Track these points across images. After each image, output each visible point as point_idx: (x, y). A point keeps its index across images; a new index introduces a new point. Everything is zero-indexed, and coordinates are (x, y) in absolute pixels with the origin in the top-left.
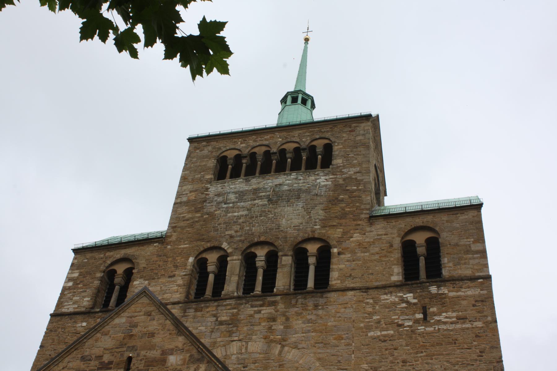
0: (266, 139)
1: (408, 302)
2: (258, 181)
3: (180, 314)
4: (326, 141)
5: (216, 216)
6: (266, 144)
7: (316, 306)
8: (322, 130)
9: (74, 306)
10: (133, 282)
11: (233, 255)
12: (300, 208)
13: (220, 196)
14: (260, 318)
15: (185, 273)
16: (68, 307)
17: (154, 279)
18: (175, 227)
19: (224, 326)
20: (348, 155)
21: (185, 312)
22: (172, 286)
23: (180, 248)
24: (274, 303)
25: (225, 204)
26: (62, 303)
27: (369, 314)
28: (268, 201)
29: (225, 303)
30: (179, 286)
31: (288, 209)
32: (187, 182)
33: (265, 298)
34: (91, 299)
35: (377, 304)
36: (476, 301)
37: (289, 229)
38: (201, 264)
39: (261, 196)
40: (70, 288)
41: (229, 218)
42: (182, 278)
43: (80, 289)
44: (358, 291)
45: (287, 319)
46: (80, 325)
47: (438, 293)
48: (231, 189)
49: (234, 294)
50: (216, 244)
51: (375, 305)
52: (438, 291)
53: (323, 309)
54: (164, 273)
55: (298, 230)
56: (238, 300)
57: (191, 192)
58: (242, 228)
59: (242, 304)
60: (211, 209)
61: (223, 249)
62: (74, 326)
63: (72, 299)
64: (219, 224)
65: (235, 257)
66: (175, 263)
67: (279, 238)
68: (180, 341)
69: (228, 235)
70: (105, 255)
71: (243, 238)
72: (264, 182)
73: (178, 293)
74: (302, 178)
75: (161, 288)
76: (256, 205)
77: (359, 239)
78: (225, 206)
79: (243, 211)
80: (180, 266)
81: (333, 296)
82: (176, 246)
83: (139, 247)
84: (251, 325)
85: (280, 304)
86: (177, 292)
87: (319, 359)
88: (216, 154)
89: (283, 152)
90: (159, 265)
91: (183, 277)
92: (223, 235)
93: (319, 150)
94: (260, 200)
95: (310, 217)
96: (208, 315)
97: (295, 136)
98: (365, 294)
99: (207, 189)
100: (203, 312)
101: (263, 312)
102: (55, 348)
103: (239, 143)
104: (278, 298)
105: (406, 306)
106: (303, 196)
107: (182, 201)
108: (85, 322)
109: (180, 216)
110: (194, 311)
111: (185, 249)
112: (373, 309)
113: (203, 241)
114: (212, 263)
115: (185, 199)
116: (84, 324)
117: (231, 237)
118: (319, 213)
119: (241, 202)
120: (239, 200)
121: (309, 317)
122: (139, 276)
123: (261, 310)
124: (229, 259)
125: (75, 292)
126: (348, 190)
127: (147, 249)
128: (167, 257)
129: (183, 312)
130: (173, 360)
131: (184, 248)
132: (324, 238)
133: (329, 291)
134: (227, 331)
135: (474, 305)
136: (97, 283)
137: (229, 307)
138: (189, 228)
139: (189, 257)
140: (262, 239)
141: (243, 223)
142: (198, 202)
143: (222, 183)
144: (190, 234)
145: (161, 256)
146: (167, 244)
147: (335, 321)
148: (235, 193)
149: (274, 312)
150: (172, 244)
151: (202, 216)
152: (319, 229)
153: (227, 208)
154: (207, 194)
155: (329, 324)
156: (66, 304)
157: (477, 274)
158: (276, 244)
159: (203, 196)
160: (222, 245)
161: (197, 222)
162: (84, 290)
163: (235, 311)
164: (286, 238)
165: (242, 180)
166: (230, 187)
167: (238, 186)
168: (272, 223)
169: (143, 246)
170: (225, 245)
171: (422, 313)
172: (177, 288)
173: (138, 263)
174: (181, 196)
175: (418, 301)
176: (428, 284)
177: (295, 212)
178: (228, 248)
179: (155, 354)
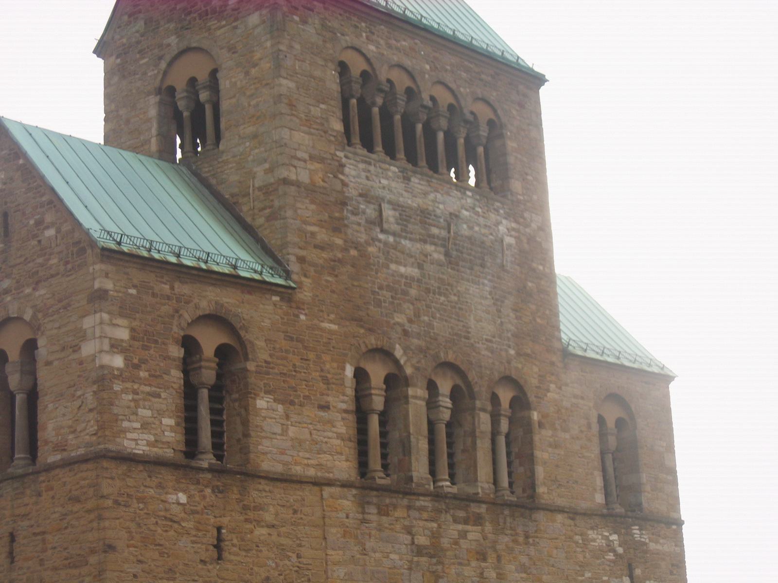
1: (614, 551)
2: (423, 188)
3: (357, 515)
5: (371, 261)
6: (410, 69)
8: (483, 76)
9: (146, 436)
10: (255, 399)
11: (415, 386)
12: (489, 296)
13: (369, 202)
14: (467, 550)
15: (344, 406)
16: (134, 435)
17: (292, 403)
19: (424, 559)
20: (527, 174)
21: (363, 513)
22: (330, 434)
23: (322, 330)
24: (478, 520)
25: (383, 231)
26: (117, 420)
27: (580, 566)
28: (447, 254)
29: (418, 504)
30: (339, 436)
31: (473, 289)
32: (298, 121)
33: (468, 503)
34: (177, 424)
35: (587, 548)
36: (673, 565)
37: (480, 342)
39: (433, 236)
40: (120, 376)
41: (393, 275)
42: (343, 419)
43: (146, 385)
44: (566, 515)
45: (499, 558)
46: (174, 497)
47: (640, 541)
48: (384, 188)
49: (429, 485)
51: (585, 550)
52: (641, 537)
53: (534, 544)
54: (307, 394)
55: (492, 352)
56: (436, 501)
57: (312, 158)
58: (417, 315)
59: (441, 512)
60: (359, 235)
61: (396, 362)
62: (163, 497)
63: (137, 415)
64: (381, 288)
66: (322, 370)
67: (471, 363)
69: (398, 324)
70: (172, 288)
71: (422, 343)
72: (432, 196)
73: (343, 457)
74: (480, 210)
75: (311, 434)
76: (429, 257)
77: (556, 396)
78: (382, 236)
79: (412, 265)
80: (333, 384)
81: (540, 516)
82: (316, 321)
83: (243, 292)
84: (460, 564)
85: (487, 524)
86: (341, 454)
90: (294, 365)
91: (345, 415)
92: (392, 322)
93: (484, 132)
94: (433, 248)
95: (502, 322)
96: (398, 527)
97: (446, 70)
98: (572, 522)
99: (342, 166)
100: (390, 518)
101: (470, 536)
102: (140, 558)
103: (364, 34)
104: (483, 509)
105: (614, 558)
107: (300, 178)
108: (184, 491)
109: (304, 226)
110: (375, 511)
111: (334, 337)
112: (585, 557)
113: (362, 327)
114: (379, 389)
115: (304, 177)
116: (183, 498)
117: (406, 333)
119: (406, 238)
120: (402, 230)
121: (524, 559)
122: (261, 384)
123: (468, 532)
124: (411, 391)
125: (135, 392)
126: (534, 270)
127: (261, 306)
128: (305, 348)
129: (360, 510)
131: (331, 332)
132: (522, 382)
133: (538, 509)
134: (430, 572)
135: (672, 573)
136: (176, 376)
137: (425, 515)
138: (330, 274)
139: (344, 363)
140: (451, 358)
141: (416, 300)
142: (332, 199)
143: (365, 162)
144: (335, 296)
145: (292, 339)
146: (298, 308)
147: (549, 574)
148: (395, 206)
149: (482, 540)
150: (307, 311)
151: (345, 250)
152: (515, 359)
153: (386, 244)
154: (344, 184)
155: (544, 577)
156: (126, 424)
157: (673, 515)
158: (470, 379)
160: (394, 349)
161: (340, 261)
162: (153, 389)
163: (435, 525)
164: (481, 367)
165: (397, 170)
166: (380, 182)
167: (394, 184)
168: (459, 320)
169: (250, 293)
170: (398, 353)
171: (629, 576)
172: (338, 442)
173: (251, 342)
174: (295, 162)
175: (624, 551)
176: (630, 520)
177: (483, 301)
178: (405, 363)
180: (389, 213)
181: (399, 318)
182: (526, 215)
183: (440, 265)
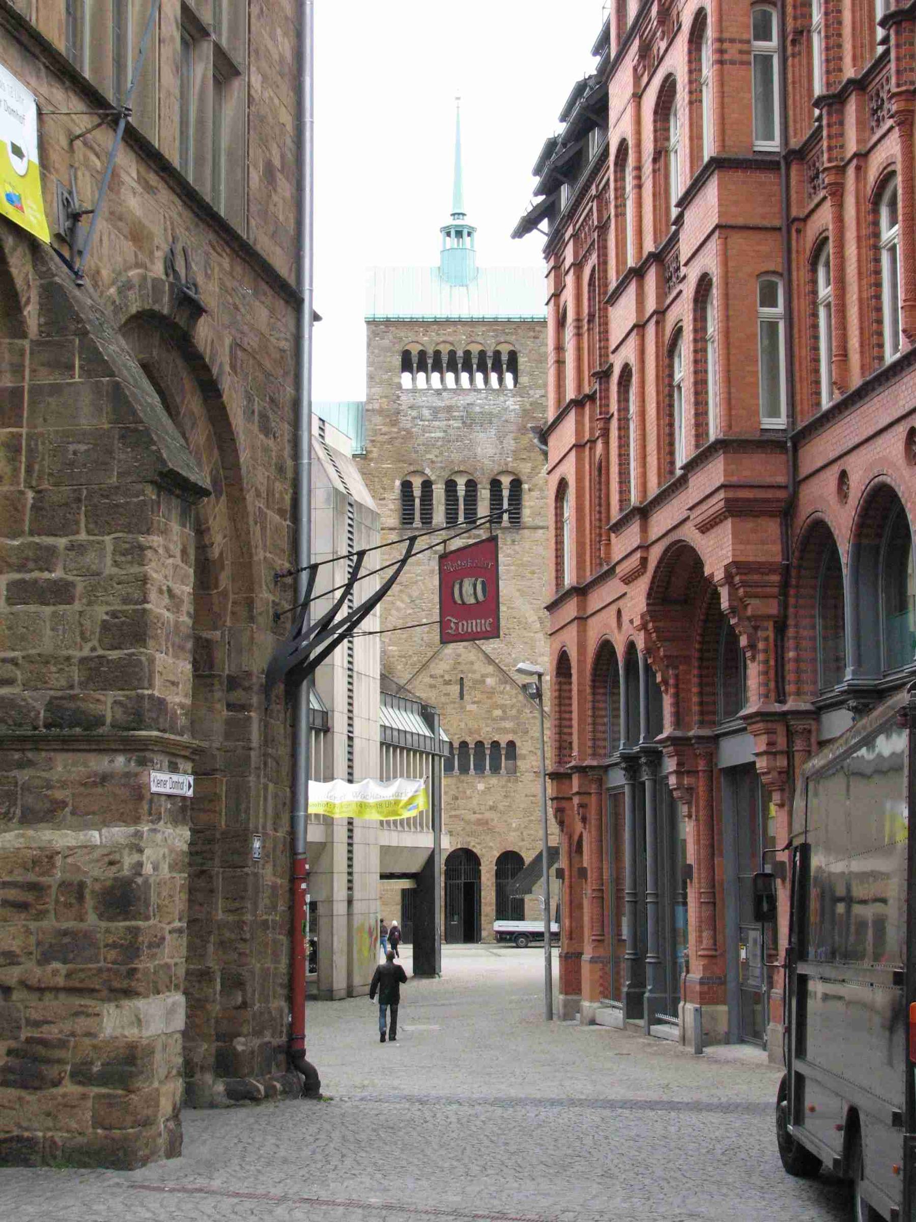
0: (447, 334)
4: (512, 348)
7: (513, 541)
18: (373, 441)
28: (464, 423)
31: (481, 435)
38: (407, 486)
50: (419, 469)
58: (441, 453)
65: (439, 486)
68: (490, 669)
81: (526, 531)
87: (519, 590)
88: (399, 348)
89: (467, 353)
99: (399, 397)
106: (495, 420)
117: (433, 462)
118: (510, 443)
130: (490, 681)
148: (429, 408)
159: (396, 406)
170: (428, 471)
179: (477, 676)
180: (426, 413)
181: (428, 456)
182: (531, 392)
183: (459, 428)
